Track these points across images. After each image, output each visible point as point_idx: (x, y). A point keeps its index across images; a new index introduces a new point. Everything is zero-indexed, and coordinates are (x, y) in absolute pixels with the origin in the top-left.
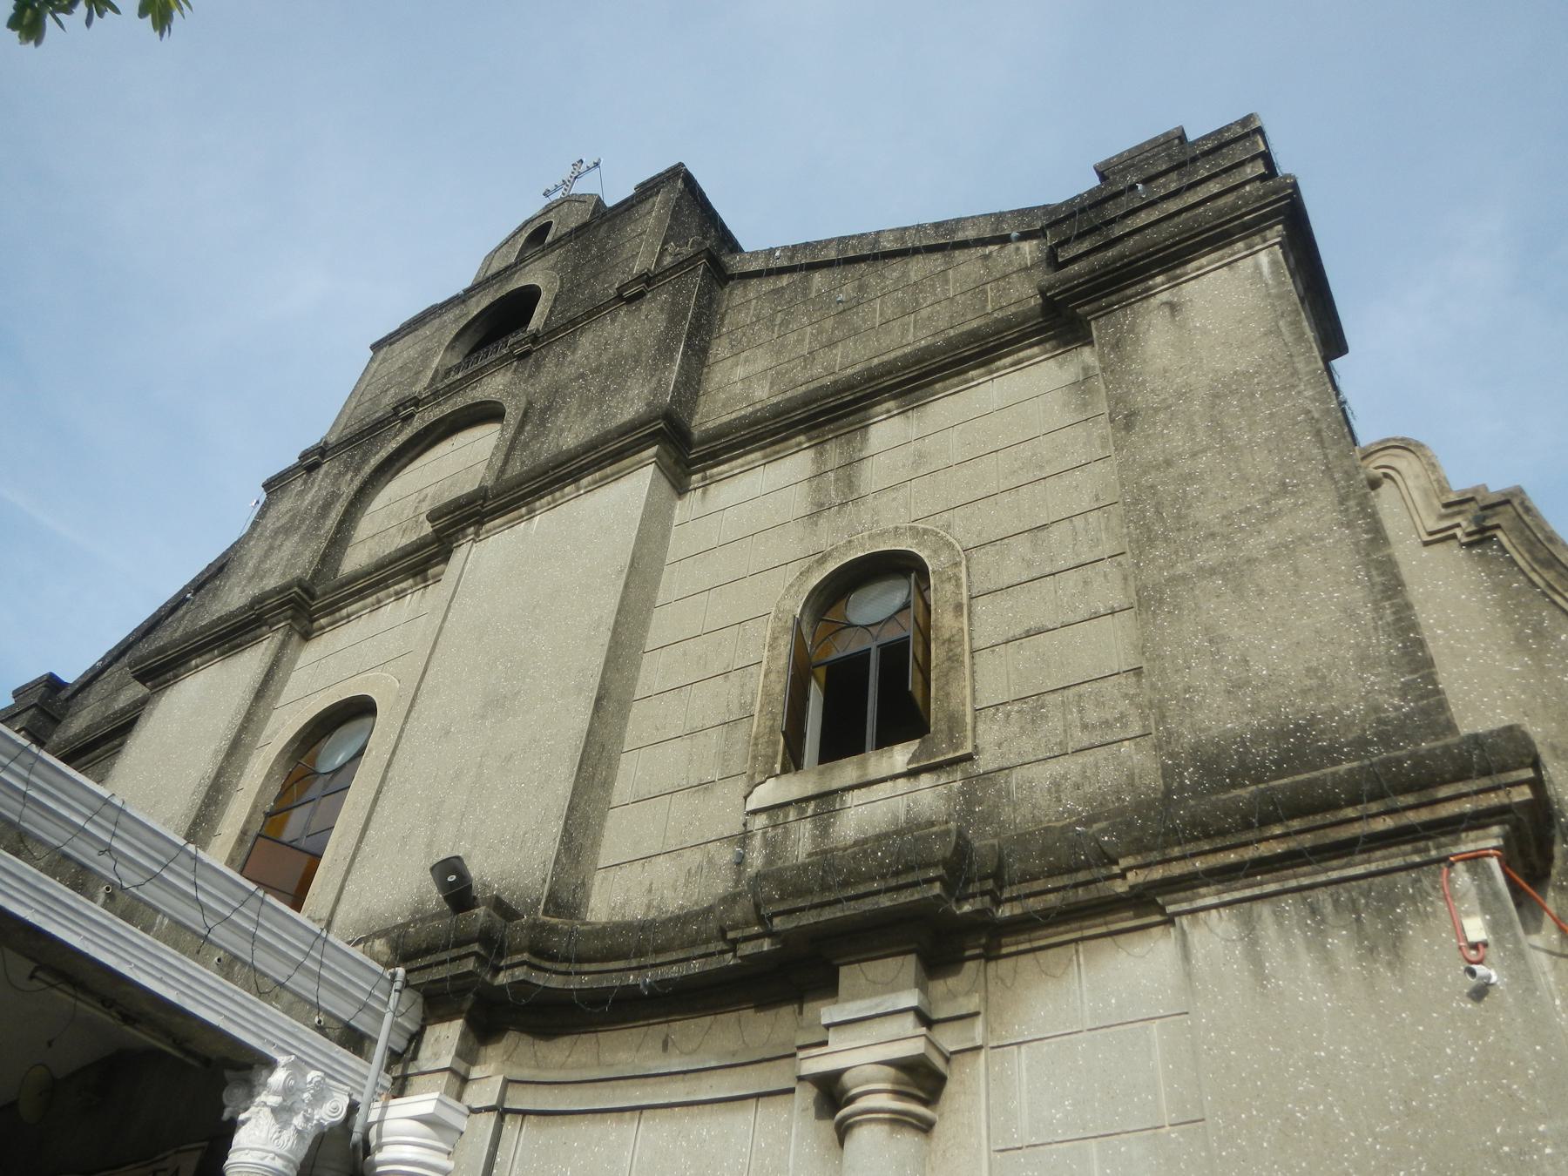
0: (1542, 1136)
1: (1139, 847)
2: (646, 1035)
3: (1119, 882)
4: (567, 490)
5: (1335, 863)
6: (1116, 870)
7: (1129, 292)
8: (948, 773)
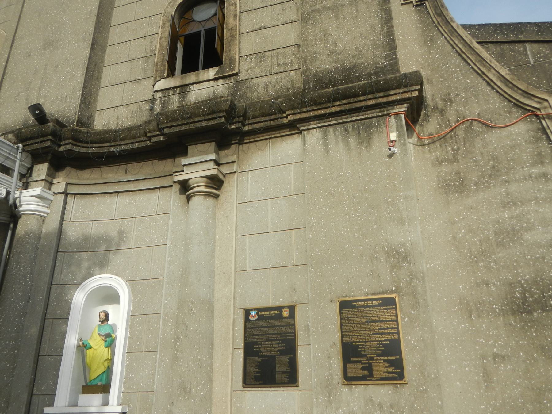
0: (401, 196)
1: (293, 108)
2: (118, 168)
3: (285, 119)
5: (355, 115)
6: (284, 115)
8: (229, 79)
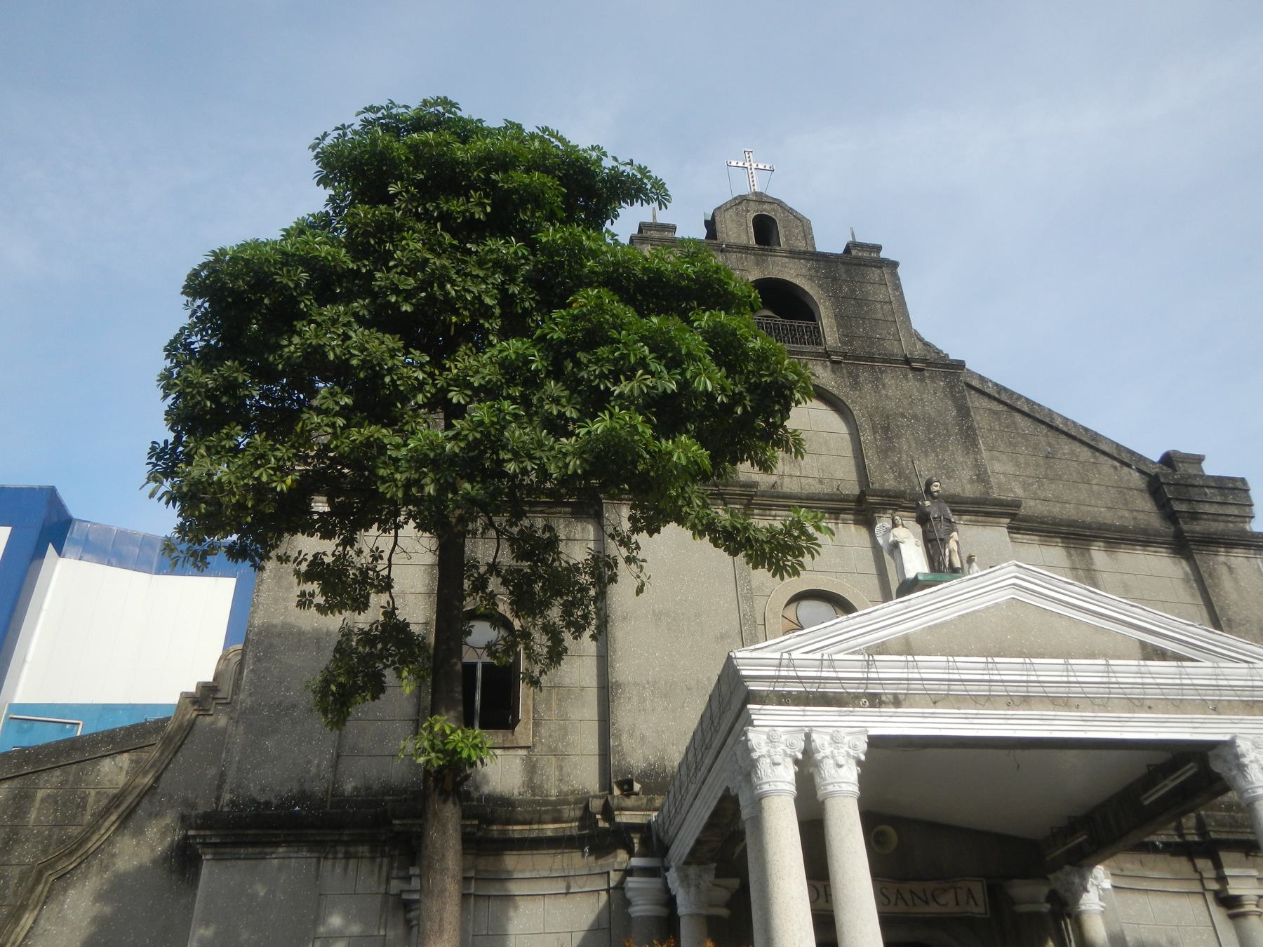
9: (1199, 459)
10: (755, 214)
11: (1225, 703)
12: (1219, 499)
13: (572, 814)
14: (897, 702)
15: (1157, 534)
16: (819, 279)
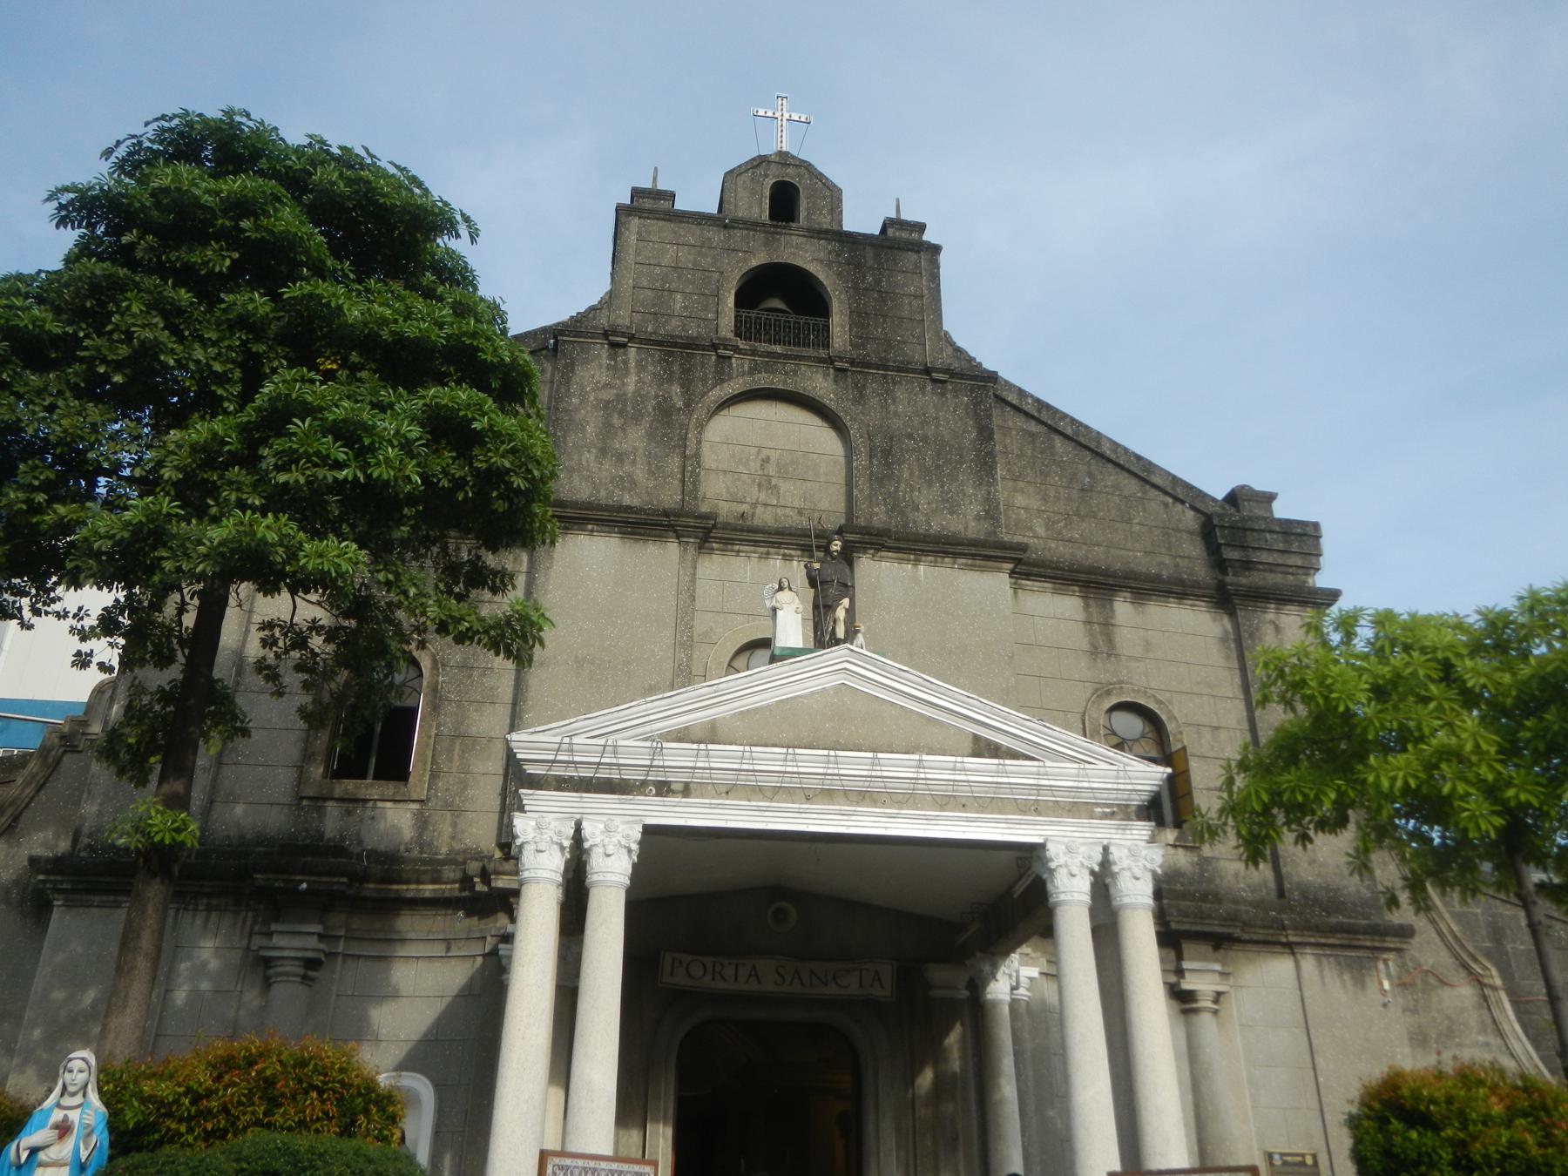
1: (1296, 928)
4: (947, 560)
7: (1259, 604)
9: (1270, 498)
10: (774, 180)
11: (1050, 804)
12: (1281, 546)
13: (452, 875)
14: (686, 790)
15: (1196, 585)
16: (840, 264)
